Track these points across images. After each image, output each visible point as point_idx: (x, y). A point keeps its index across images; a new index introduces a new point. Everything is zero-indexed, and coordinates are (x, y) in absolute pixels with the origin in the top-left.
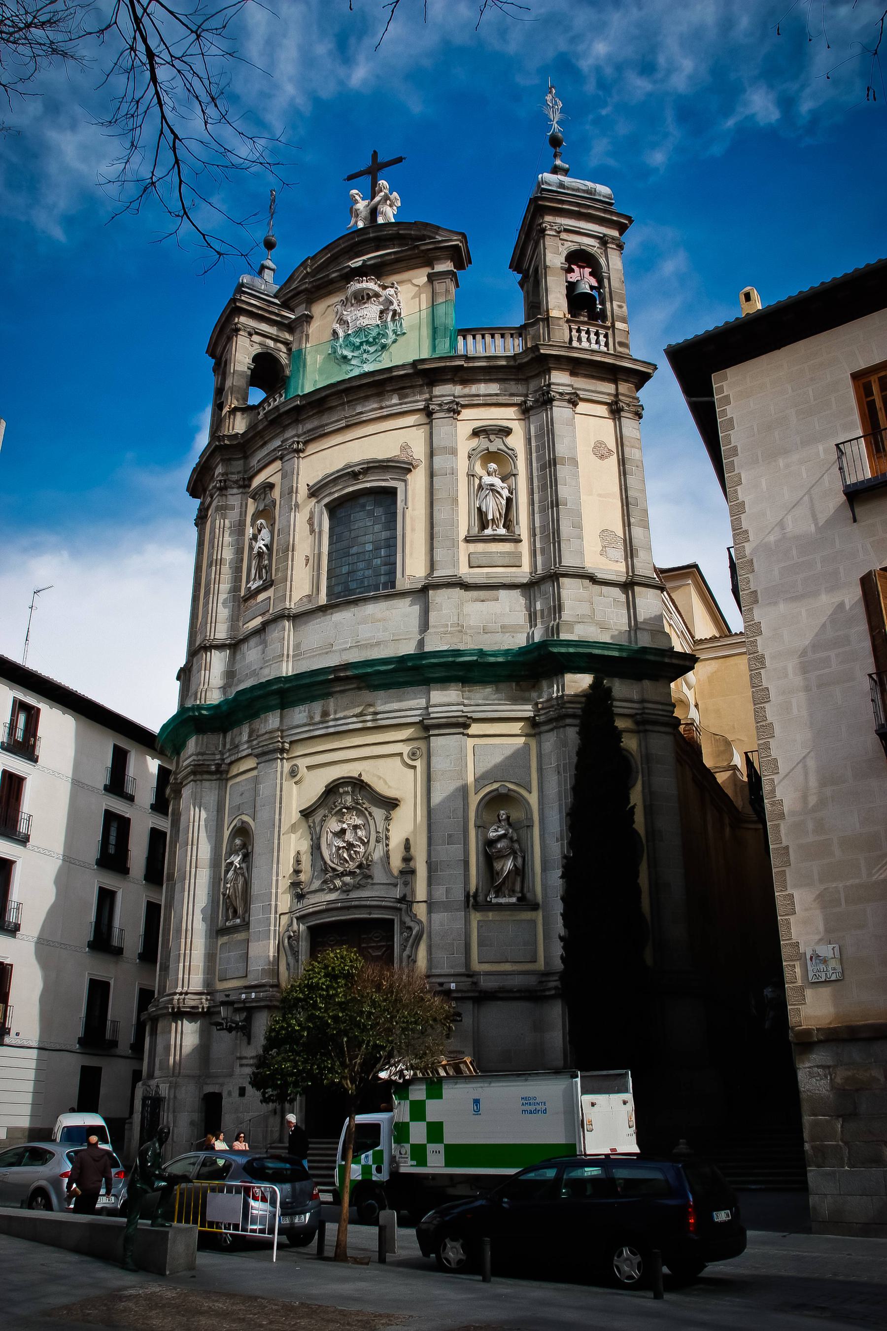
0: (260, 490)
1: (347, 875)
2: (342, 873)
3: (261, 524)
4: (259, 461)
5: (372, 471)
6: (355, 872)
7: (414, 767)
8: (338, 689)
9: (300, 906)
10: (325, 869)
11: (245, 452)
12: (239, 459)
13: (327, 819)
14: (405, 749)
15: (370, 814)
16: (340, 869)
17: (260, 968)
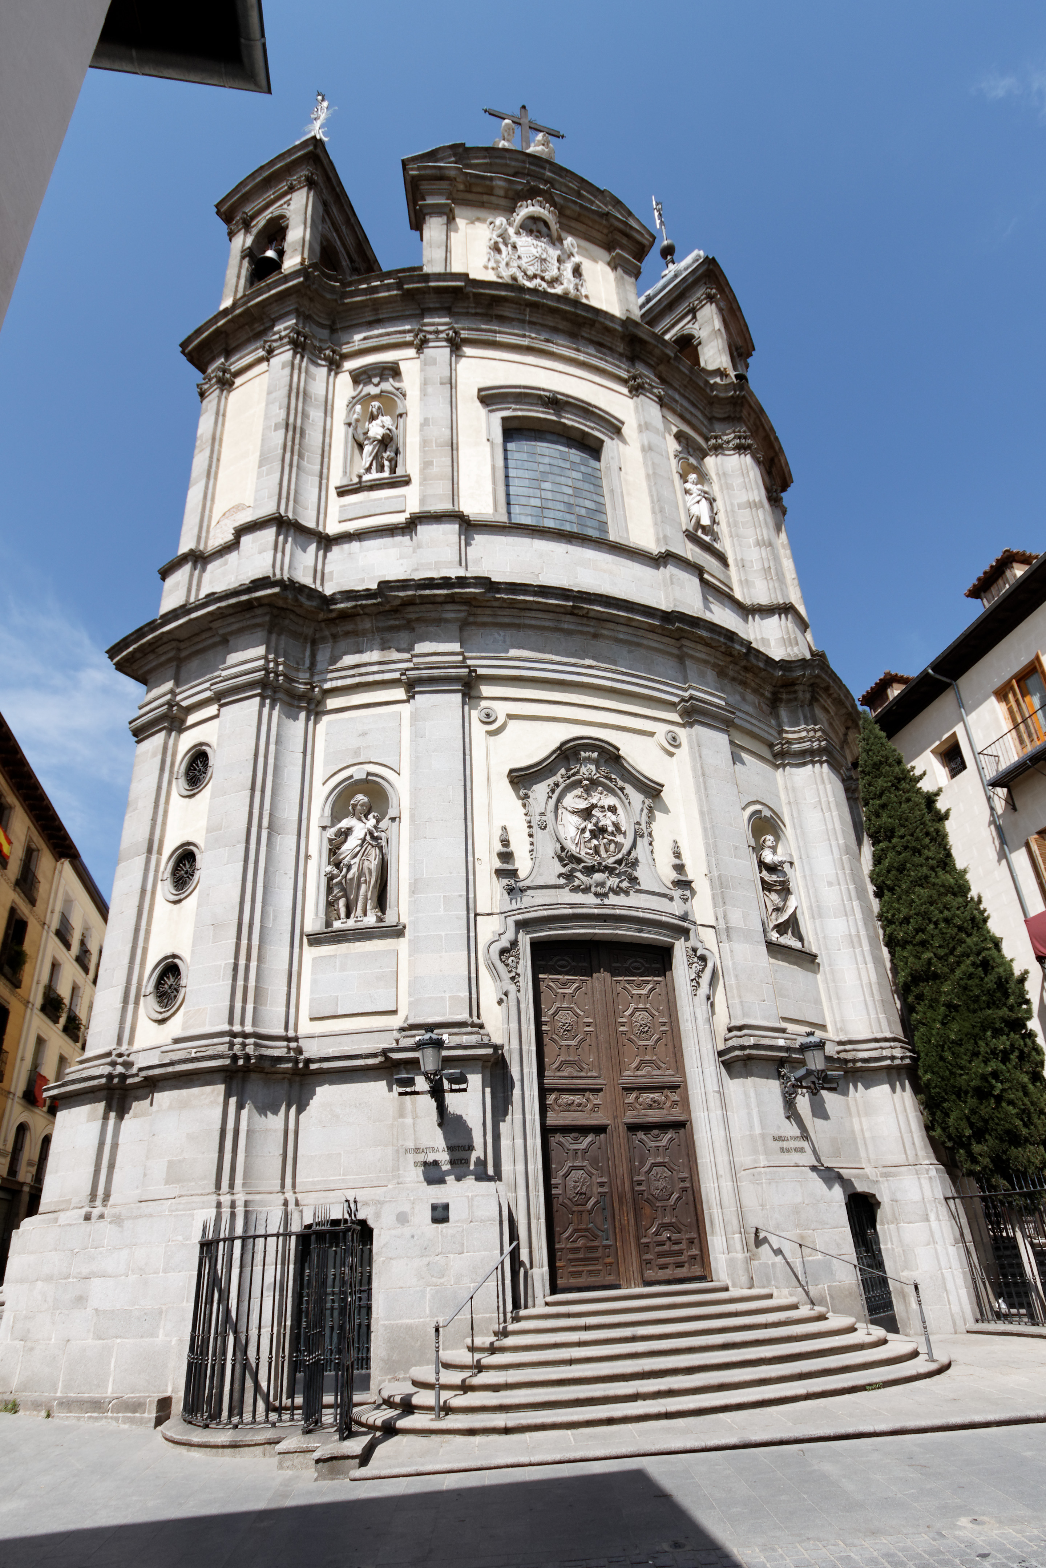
0: (374, 369)
1: (599, 871)
2: (594, 866)
3: (379, 408)
4: (365, 339)
5: (568, 408)
6: (615, 869)
7: (671, 755)
8: (566, 626)
9: (514, 906)
10: (566, 857)
11: (334, 323)
12: (323, 326)
13: (558, 791)
14: (661, 729)
15: (626, 796)
16: (590, 862)
17: (447, 995)
